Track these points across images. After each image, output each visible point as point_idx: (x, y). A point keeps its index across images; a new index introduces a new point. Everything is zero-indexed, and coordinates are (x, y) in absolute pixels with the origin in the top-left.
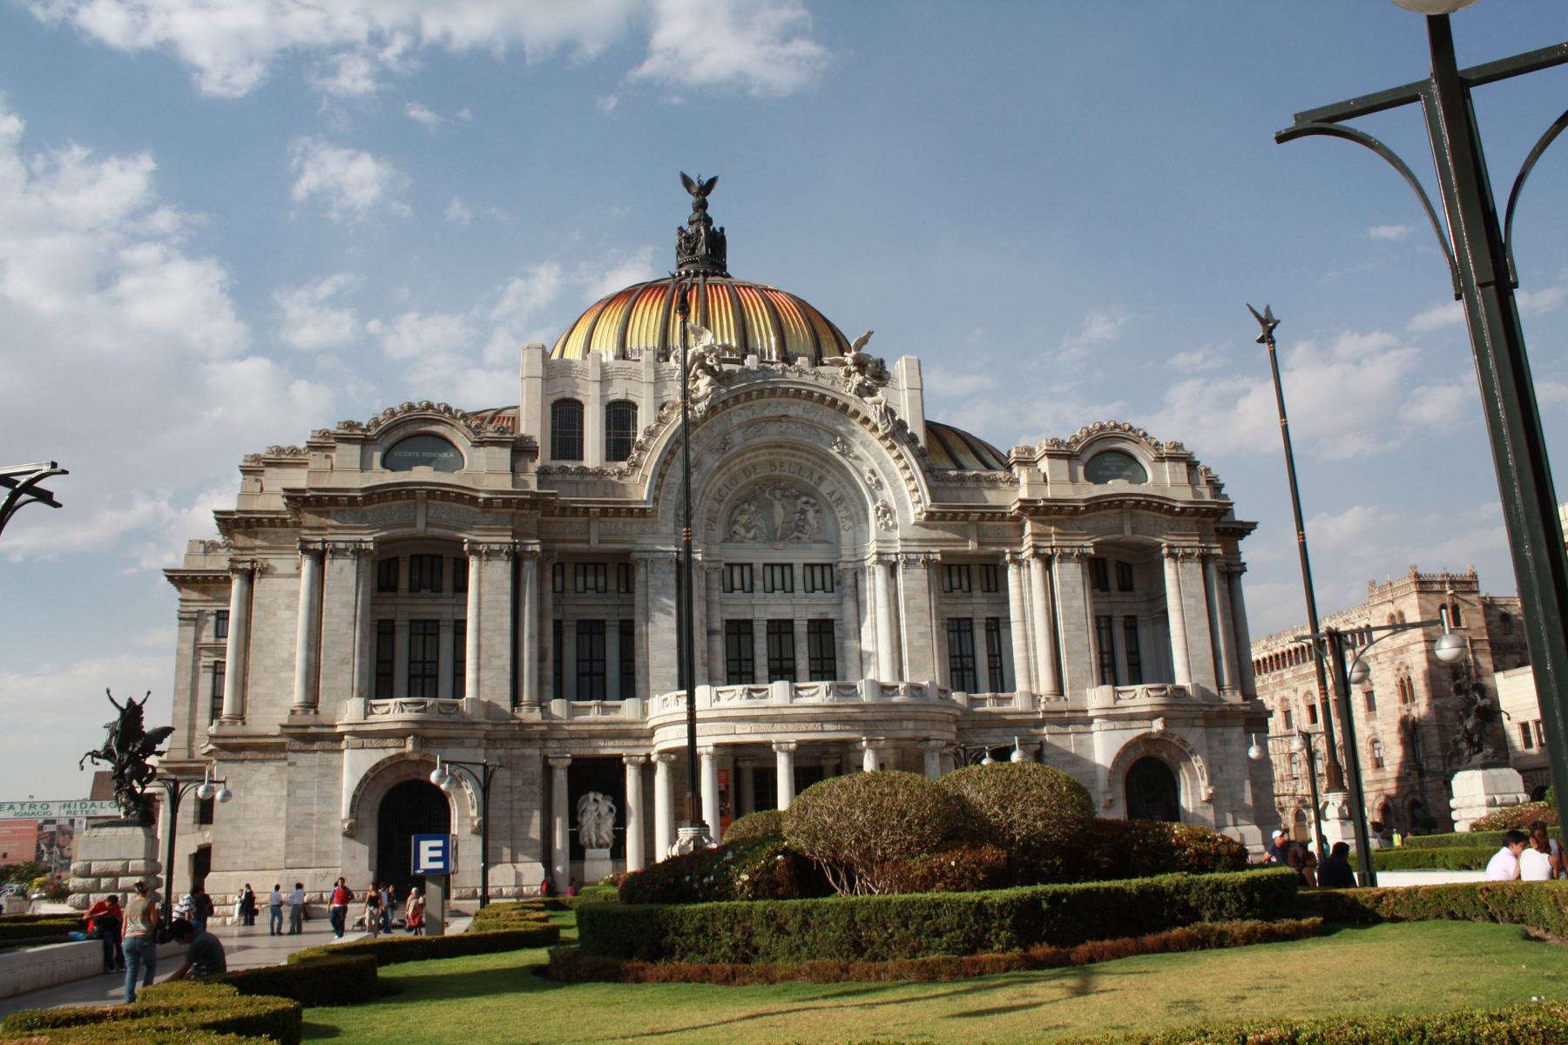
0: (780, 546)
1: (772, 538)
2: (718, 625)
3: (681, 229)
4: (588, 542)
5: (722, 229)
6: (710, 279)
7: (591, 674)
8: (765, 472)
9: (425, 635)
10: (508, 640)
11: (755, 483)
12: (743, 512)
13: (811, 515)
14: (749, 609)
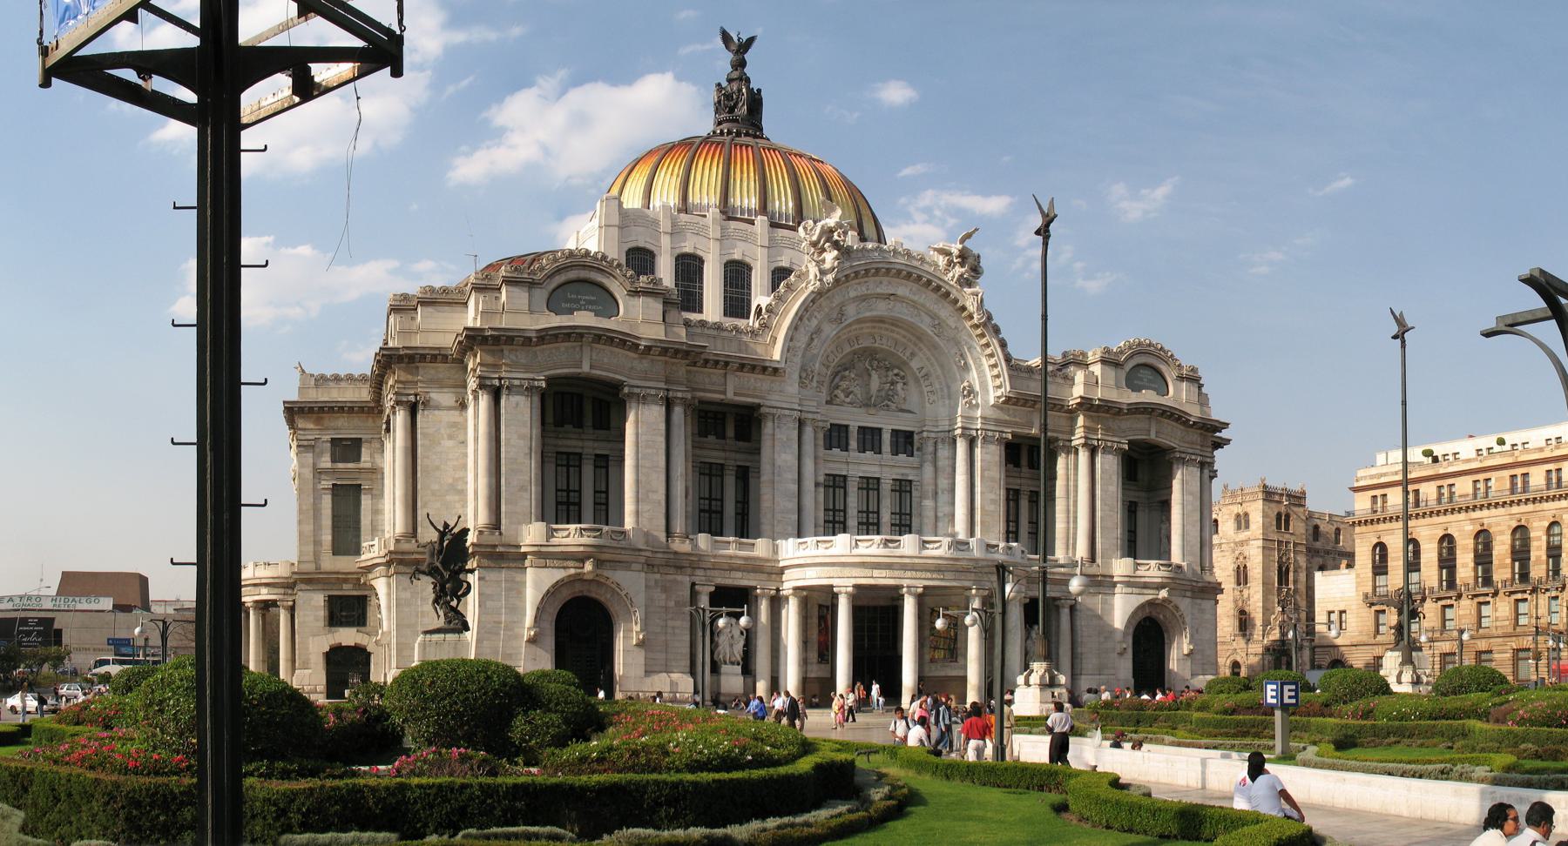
0: (872, 411)
1: (867, 406)
2: (821, 479)
3: (719, 85)
4: (724, 393)
5: (759, 91)
6: (744, 140)
7: (710, 511)
8: (865, 343)
9: (568, 466)
10: (663, 477)
11: (854, 353)
12: (843, 378)
13: (899, 386)
14: (844, 466)
